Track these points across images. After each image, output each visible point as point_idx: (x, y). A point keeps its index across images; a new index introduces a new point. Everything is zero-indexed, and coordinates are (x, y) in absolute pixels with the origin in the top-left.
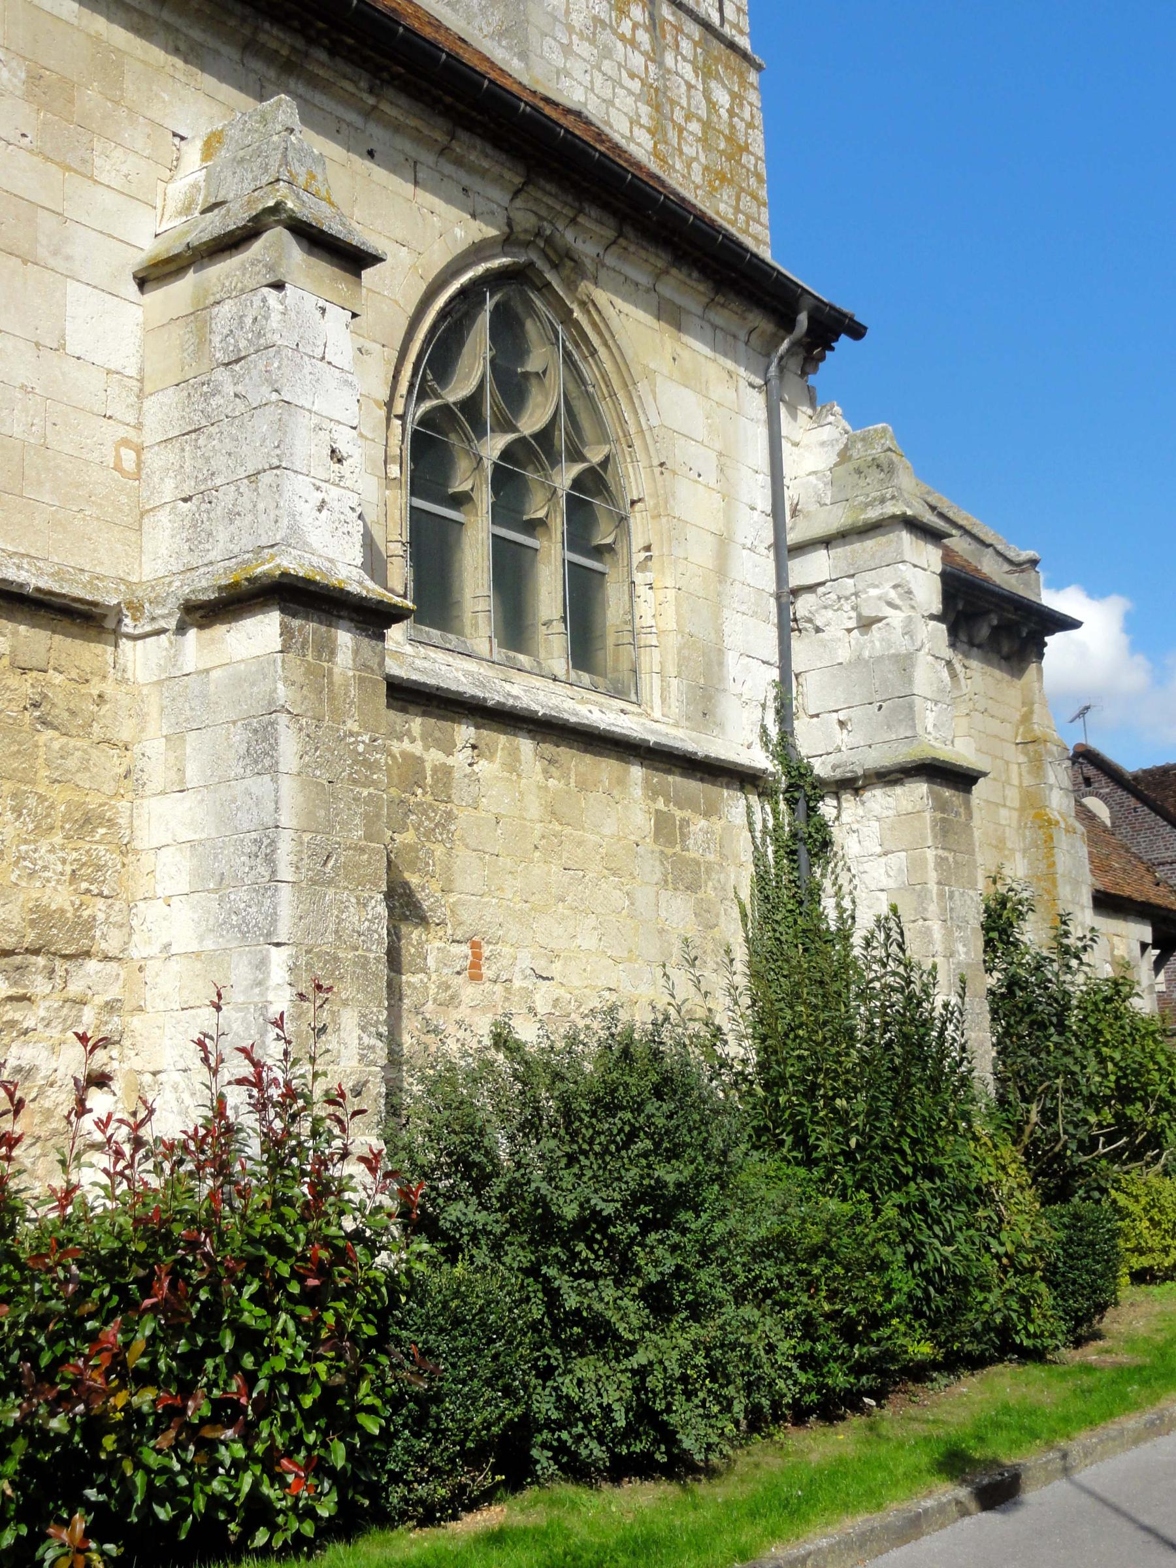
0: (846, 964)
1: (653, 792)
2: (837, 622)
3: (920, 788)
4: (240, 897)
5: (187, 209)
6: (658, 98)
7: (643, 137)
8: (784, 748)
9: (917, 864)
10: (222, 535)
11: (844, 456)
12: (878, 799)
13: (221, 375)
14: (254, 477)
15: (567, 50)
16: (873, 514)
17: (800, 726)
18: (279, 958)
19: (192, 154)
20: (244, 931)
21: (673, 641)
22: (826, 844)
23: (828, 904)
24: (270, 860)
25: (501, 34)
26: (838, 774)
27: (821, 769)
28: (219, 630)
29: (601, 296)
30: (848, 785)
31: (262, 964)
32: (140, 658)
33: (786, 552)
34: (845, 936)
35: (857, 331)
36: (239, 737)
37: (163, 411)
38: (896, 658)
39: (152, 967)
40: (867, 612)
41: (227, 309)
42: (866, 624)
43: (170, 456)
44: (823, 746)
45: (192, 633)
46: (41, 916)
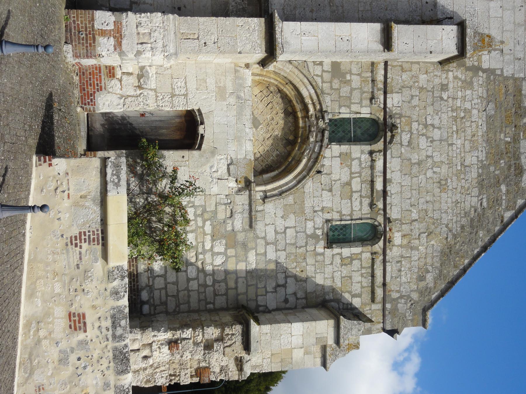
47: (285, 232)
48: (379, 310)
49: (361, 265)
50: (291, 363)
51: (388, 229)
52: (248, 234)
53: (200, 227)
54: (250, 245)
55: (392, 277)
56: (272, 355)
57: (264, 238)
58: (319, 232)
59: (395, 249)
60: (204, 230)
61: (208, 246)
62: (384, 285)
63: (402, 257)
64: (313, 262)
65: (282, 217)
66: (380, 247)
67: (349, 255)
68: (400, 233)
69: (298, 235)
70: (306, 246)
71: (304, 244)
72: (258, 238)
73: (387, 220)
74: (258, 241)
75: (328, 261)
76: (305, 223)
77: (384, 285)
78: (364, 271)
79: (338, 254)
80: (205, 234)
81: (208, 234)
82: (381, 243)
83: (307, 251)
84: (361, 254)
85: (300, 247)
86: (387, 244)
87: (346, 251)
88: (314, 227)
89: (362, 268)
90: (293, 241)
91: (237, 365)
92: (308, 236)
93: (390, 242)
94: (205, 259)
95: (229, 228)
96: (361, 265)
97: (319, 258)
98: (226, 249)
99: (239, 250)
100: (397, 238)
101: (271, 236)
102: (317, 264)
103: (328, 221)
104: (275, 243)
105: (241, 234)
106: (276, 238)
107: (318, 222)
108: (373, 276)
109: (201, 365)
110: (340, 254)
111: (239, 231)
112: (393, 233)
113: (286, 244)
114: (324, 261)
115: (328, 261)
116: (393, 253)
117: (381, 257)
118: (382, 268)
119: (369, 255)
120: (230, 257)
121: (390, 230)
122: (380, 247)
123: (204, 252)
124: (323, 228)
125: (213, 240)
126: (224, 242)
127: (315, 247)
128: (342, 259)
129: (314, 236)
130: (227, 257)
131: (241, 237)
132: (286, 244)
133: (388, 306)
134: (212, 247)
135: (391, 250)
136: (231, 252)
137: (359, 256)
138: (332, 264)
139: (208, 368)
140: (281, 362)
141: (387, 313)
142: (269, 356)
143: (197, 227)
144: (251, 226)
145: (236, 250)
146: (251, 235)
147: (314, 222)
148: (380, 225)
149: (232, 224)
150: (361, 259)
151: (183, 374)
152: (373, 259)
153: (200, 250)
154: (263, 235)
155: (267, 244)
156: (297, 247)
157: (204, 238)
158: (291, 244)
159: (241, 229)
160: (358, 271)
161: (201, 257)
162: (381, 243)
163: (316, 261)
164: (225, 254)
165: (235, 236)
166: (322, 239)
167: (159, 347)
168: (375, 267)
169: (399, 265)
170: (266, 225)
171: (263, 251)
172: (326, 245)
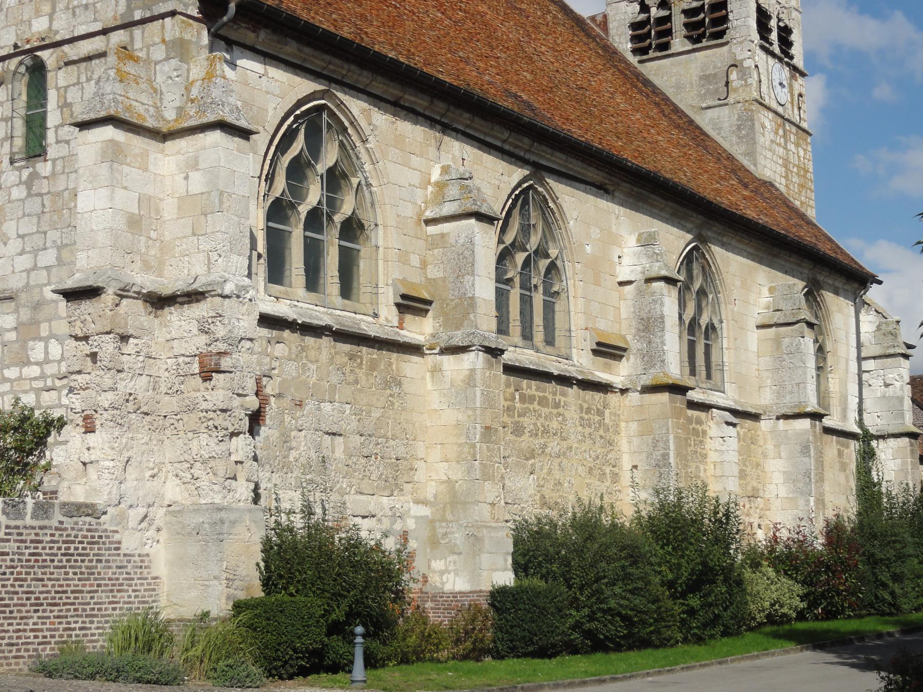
0: (880, 493)
1: (838, 443)
2: (877, 383)
3: (906, 440)
4: (800, 485)
5: (768, 308)
6: (786, 164)
7: (783, 181)
8: (860, 423)
9: (904, 463)
10: (788, 397)
11: (879, 328)
12: (892, 442)
13: (785, 356)
14: (798, 385)
15: (765, 157)
16: (891, 351)
17: (865, 416)
18: (812, 499)
19: (765, 291)
20: (802, 493)
21: (838, 395)
22: (874, 454)
23: (874, 473)
24: (809, 477)
25: (746, 154)
26: (879, 433)
27: (872, 431)
28: (791, 421)
29: (824, 292)
30: (883, 437)
31: (808, 501)
32: (765, 425)
33: (860, 359)
34: (880, 484)
35: (880, 282)
36: (798, 448)
37: (766, 362)
38: (898, 398)
39: (772, 501)
40: (888, 382)
41: (787, 340)
42: (887, 385)
43: (769, 374)
44: (873, 423)
45: (781, 421)
46: (754, 489)
47: (21, 237)
48: (143, 33)
49: (74, 85)
50: (209, 193)
51: (28, 47)
52: (22, 302)
53: (12, 387)
54: (36, 299)
55: (95, 20)
56: (194, 234)
57: (28, 271)
58: (26, 173)
59: (56, 26)
60: (15, 380)
61: (35, 371)
62: (105, 32)
63: (67, 8)
64: (63, 177)
65: (5, 244)
66: (52, 55)
67: (58, 112)
68: (34, 22)
69: (27, 211)
70: (40, 195)
71: (39, 199)
72: (28, 283)
73: (17, 52)
74: (32, 283)
75: (63, 150)
76: (13, 201)
77: (105, 32)
78: (83, 78)
79: (56, 132)
80: (20, 378)
81: (21, 372)
82: (44, 55)
83: (49, 193)
84: (58, 89)
85: (43, 206)
86: (47, 42)
87: (53, 118)
88: (18, 185)
89: (78, 83)
90: (35, 220)
91: (198, 301)
92: (29, 195)
93: (43, 39)
94: (52, 376)
95: (12, 336)
96: (74, 85)
97: (59, 168)
98: (40, 339)
99: (41, 316)
100: (40, 25)
101: (24, 262)
102: (67, 171)
103: (12, 162)
104: (35, 252)
105: (21, 313)
106: (29, 252)
107: (13, 178)
108: (89, 58)
109: (197, 371)
110: (57, 127)
111: (17, 319)
112: (33, 35)
113: (38, 232)
114: (63, 158)
115: (63, 150)
116: (63, 28)
117: (66, 48)
118: (82, 43)
119: (61, 73)
120: (50, 331)
121: (28, 42)
122: (52, 55)
123: (43, 376)
124: (20, 169)
125: (28, 363)
126: (31, 343)
127: (45, 178)
128: (62, 125)
129: (29, 184)
130: (52, 336)
131: (25, 314)
132: (38, 232)
133: (138, 15)
134: (37, 364)
135: (57, 32)
136: (44, 331)
137: (62, 91)
138: (67, 142)
139: (201, 355)
140: (206, 215)
141: (148, 15)
142: (195, 238)
143: (11, 391)
144: (10, 298)
145: (42, 322)
146: (23, 296)
147: (13, 186)
148: (21, 63)
149: (9, 330)
150: (66, 87)
151: (204, 406)
152: (67, 64)
153: (39, 384)
154: (24, 275)
155: (35, 267)
156: (43, 212)
157: (26, 379)
158: (39, 223)
159: (15, 316)
160: (83, 87)
161: (49, 383)
162: (44, 55)
163: (63, 173)
164: (46, 340)
165: (23, 324)
166: (34, 167)
167: (88, 449)
168: (75, 58)
169: (78, 11)
170: (13, 272)
171: (44, 273)
172: (42, 158)
